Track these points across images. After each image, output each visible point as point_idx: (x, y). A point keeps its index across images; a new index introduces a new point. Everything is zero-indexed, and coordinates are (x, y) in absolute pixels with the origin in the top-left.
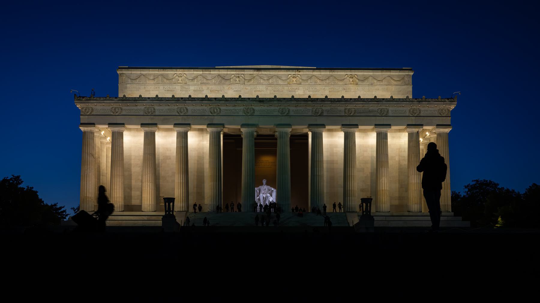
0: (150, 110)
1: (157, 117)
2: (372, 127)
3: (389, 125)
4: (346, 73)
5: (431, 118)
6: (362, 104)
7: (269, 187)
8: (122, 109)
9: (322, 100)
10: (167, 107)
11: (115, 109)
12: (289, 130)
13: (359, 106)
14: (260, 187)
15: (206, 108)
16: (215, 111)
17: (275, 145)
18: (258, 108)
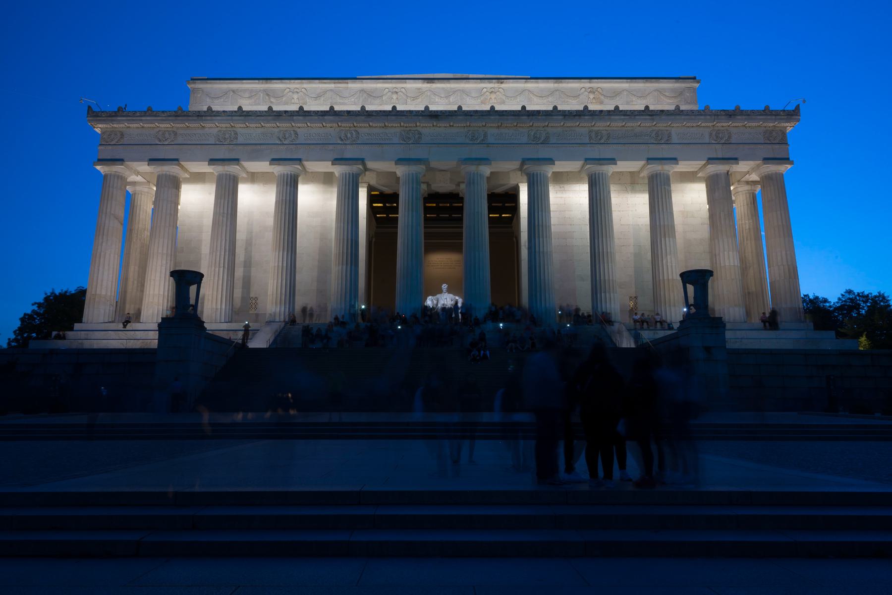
0: (227, 136)
1: (240, 147)
2: (642, 163)
3: (674, 160)
4: (582, 85)
5: (752, 146)
6: (623, 120)
7: (451, 295)
8: (176, 134)
9: (546, 113)
10: (260, 130)
11: (163, 134)
12: (486, 170)
13: (617, 124)
14: (438, 296)
15: (330, 129)
16: (349, 135)
17: (460, 210)
18: (427, 129)
